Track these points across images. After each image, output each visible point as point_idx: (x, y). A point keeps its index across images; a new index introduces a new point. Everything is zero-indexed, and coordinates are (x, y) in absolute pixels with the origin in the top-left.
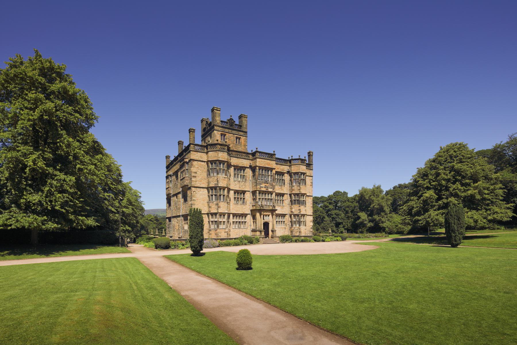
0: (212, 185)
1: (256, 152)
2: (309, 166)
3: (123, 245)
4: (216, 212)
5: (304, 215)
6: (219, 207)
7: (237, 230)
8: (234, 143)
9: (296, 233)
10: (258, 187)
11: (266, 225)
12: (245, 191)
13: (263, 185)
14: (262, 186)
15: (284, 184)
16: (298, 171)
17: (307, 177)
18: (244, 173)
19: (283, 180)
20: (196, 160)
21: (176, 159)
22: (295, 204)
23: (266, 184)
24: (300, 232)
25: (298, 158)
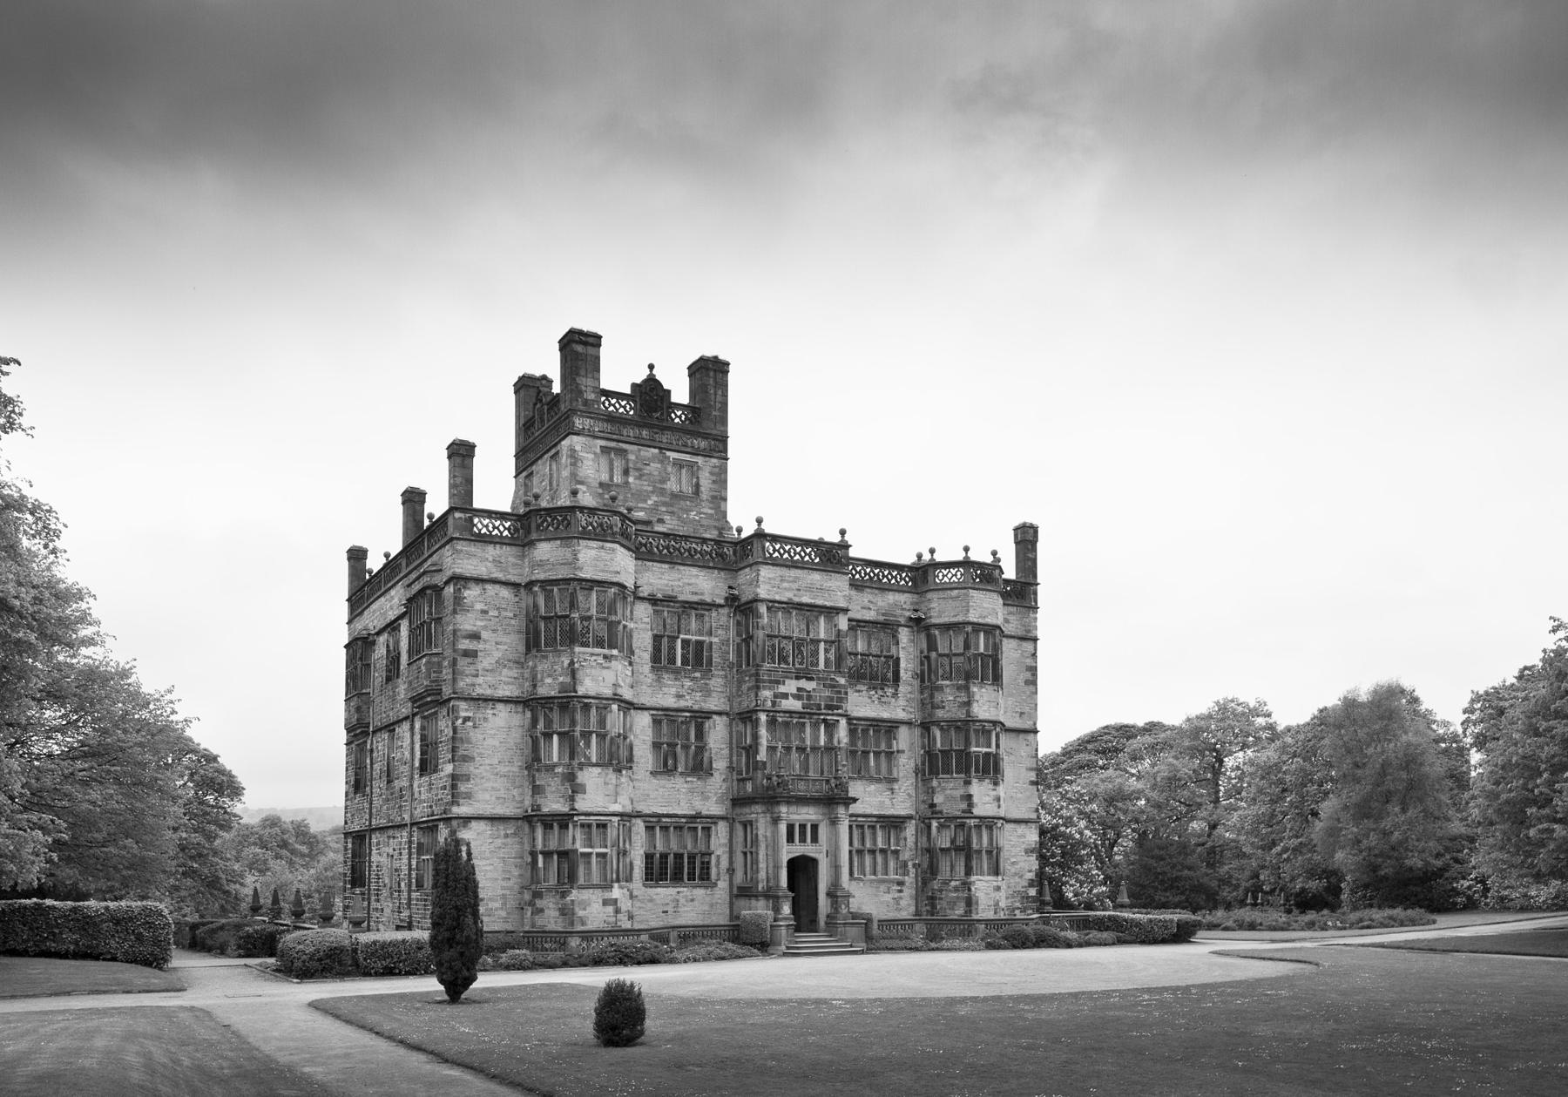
1: (760, 535)
2: (1022, 593)
3: (156, 961)
4: (566, 809)
5: (989, 823)
6: (577, 789)
8: (662, 492)
10: (766, 694)
11: (802, 869)
12: (708, 715)
13: (791, 686)
14: (782, 689)
15: (897, 678)
16: (960, 619)
17: (1005, 641)
20: (479, 581)
21: (392, 565)
22: (947, 771)
23: (803, 683)
24: (969, 902)
25: (960, 556)
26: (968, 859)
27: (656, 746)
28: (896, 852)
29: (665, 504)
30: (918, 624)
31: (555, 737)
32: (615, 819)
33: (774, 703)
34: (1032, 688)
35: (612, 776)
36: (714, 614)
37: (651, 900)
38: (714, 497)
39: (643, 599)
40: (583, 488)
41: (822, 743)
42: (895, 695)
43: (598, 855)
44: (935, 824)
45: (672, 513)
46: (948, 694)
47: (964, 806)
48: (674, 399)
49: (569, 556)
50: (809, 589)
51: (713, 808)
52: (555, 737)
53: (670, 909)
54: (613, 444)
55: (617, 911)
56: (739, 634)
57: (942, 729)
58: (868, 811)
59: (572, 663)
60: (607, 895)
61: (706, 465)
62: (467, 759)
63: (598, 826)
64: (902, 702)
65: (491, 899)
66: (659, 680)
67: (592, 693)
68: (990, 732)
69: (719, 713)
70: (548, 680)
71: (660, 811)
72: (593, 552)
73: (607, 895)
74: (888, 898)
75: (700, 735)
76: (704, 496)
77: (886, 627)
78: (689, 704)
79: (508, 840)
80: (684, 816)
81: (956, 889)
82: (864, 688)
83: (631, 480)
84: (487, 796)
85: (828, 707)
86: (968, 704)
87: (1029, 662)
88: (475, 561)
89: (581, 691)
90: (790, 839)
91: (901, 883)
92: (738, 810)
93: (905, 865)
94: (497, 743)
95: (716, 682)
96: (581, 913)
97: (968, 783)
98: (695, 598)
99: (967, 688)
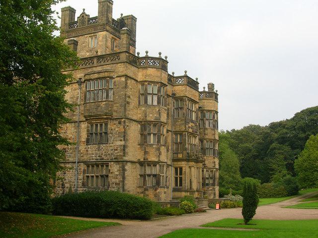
4: (157, 160)
9: (210, 195)
31: (152, 135)
44: (205, 170)
52: (152, 135)
56: (174, 106)
57: (207, 142)
70: (151, 115)
81: (211, 190)
92: (175, 163)
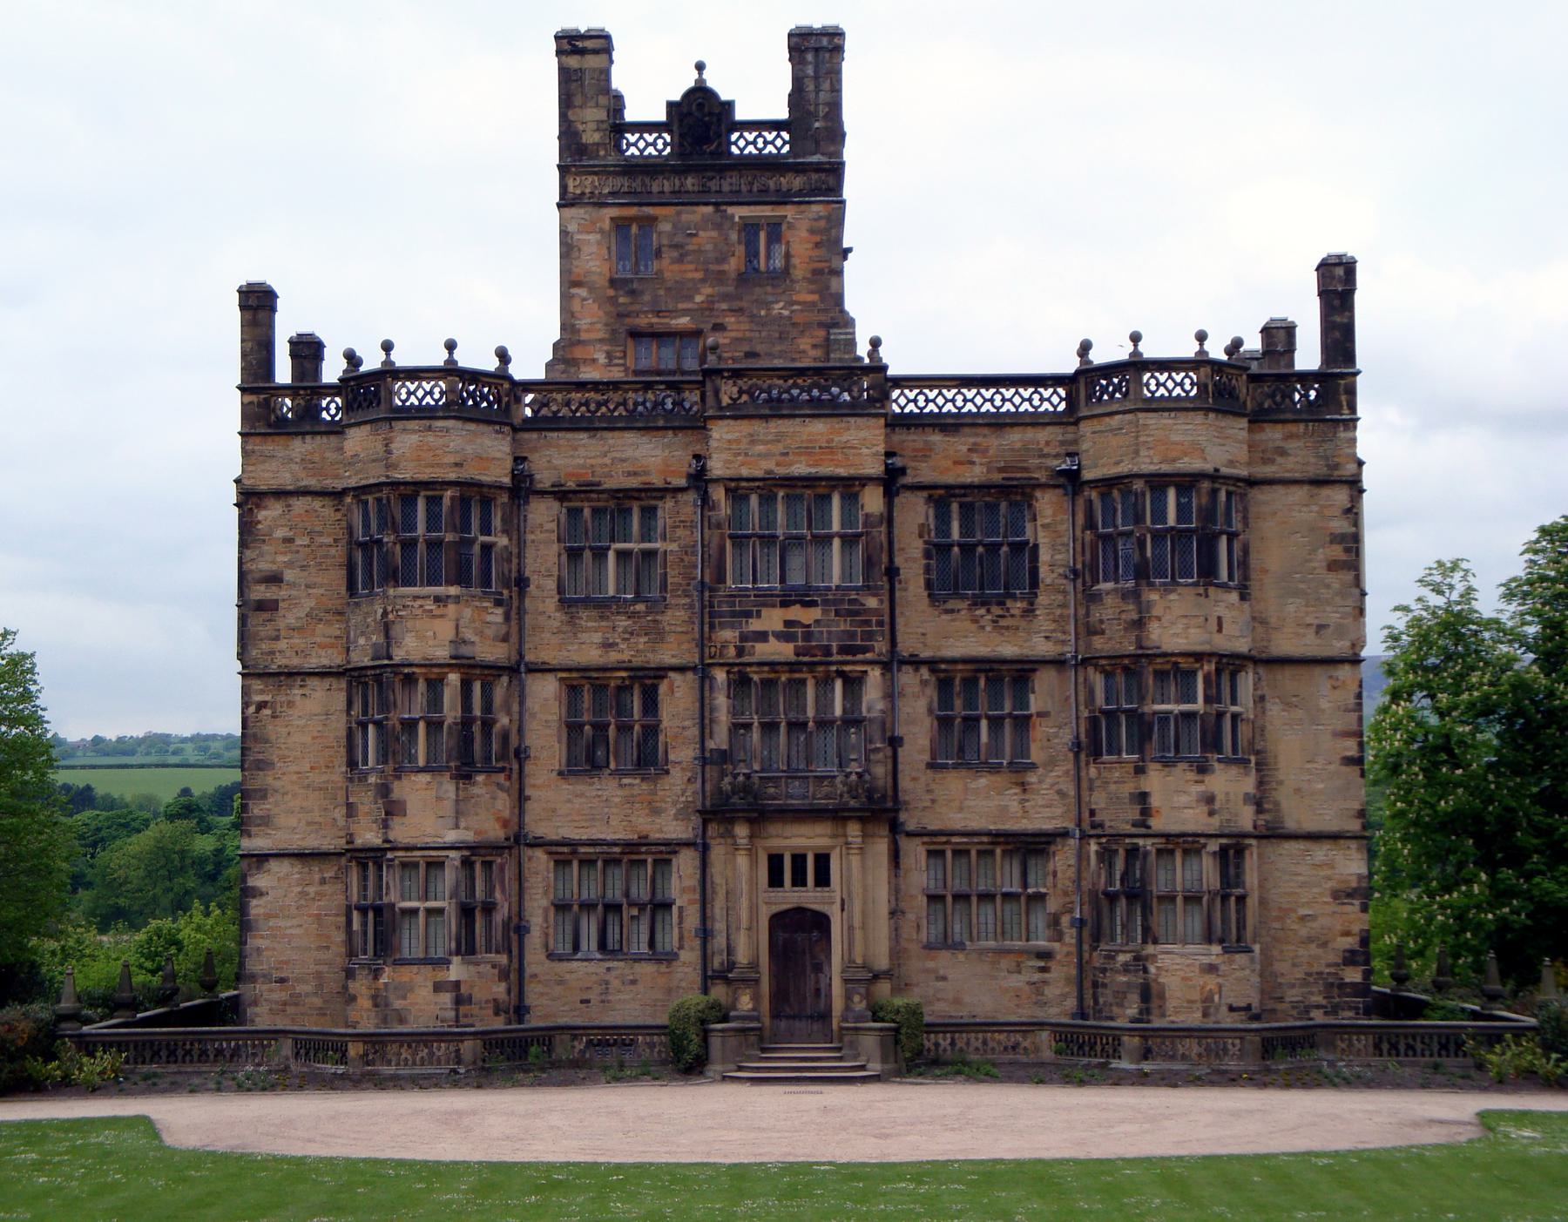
0: (361, 658)
6: (392, 809)
7: (585, 971)
8: (720, 277)
9: (1121, 996)
12: (661, 672)
13: (773, 619)
14: (755, 625)
15: (1035, 582)
18: (646, 536)
19: (1018, 548)
23: (795, 613)
24: (1147, 994)
26: (1147, 911)
27: (573, 729)
28: (1040, 898)
29: (726, 297)
30: (1071, 481)
32: (452, 854)
33: (740, 652)
34: (1348, 577)
35: (449, 788)
36: (669, 503)
37: (561, 982)
38: (816, 272)
39: (542, 493)
40: (583, 292)
41: (838, 712)
42: (1029, 612)
43: (429, 911)
45: (741, 310)
46: (1111, 609)
47: (1134, 813)
48: (740, 115)
49: (380, 448)
50: (806, 451)
51: (674, 829)
53: (592, 996)
54: (633, 211)
55: (459, 1001)
57: (1103, 671)
58: (975, 824)
59: (385, 613)
60: (441, 976)
61: (799, 221)
62: (263, 765)
63: (429, 864)
64: (1043, 622)
65: (299, 980)
66: (572, 620)
67: (416, 657)
68: (1194, 673)
69: (681, 669)
70: (362, 641)
71: (575, 834)
72: (415, 438)
73: (441, 976)
74: (1017, 981)
75: (651, 704)
76: (799, 272)
77: (1012, 492)
78: (625, 657)
79: (326, 887)
80: (614, 844)
81: (1126, 968)
82: (963, 605)
83: (665, 262)
84: (293, 822)
85: (843, 650)
86: (1139, 624)
87: (1341, 526)
88: (272, 465)
89: (399, 655)
90: (775, 880)
91: (1045, 955)
93: (1055, 921)
94: (307, 739)
95: (677, 617)
96: (398, 1004)
97: (1140, 770)
98: (633, 483)
99: (1135, 595)
